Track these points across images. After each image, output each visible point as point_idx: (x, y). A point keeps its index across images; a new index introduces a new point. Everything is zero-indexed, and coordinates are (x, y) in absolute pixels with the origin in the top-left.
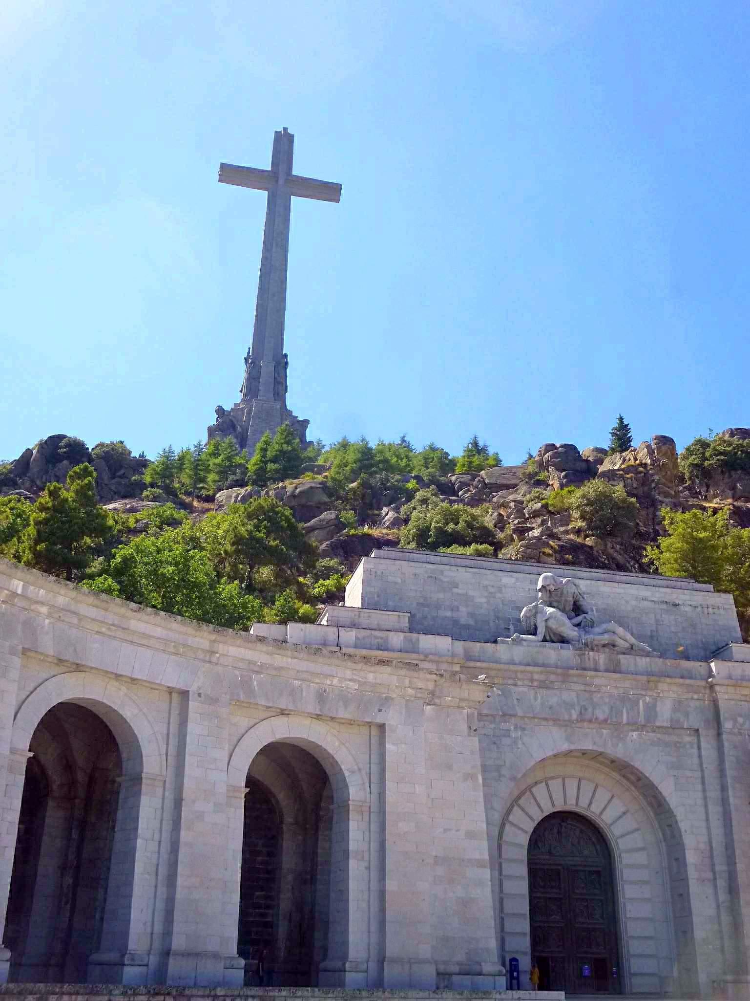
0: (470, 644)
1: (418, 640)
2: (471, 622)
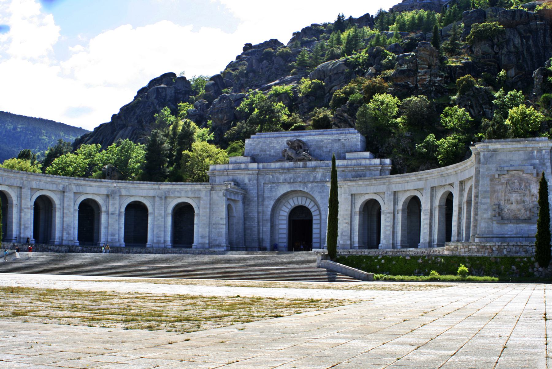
0: (264, 164)
2: (274, 154)
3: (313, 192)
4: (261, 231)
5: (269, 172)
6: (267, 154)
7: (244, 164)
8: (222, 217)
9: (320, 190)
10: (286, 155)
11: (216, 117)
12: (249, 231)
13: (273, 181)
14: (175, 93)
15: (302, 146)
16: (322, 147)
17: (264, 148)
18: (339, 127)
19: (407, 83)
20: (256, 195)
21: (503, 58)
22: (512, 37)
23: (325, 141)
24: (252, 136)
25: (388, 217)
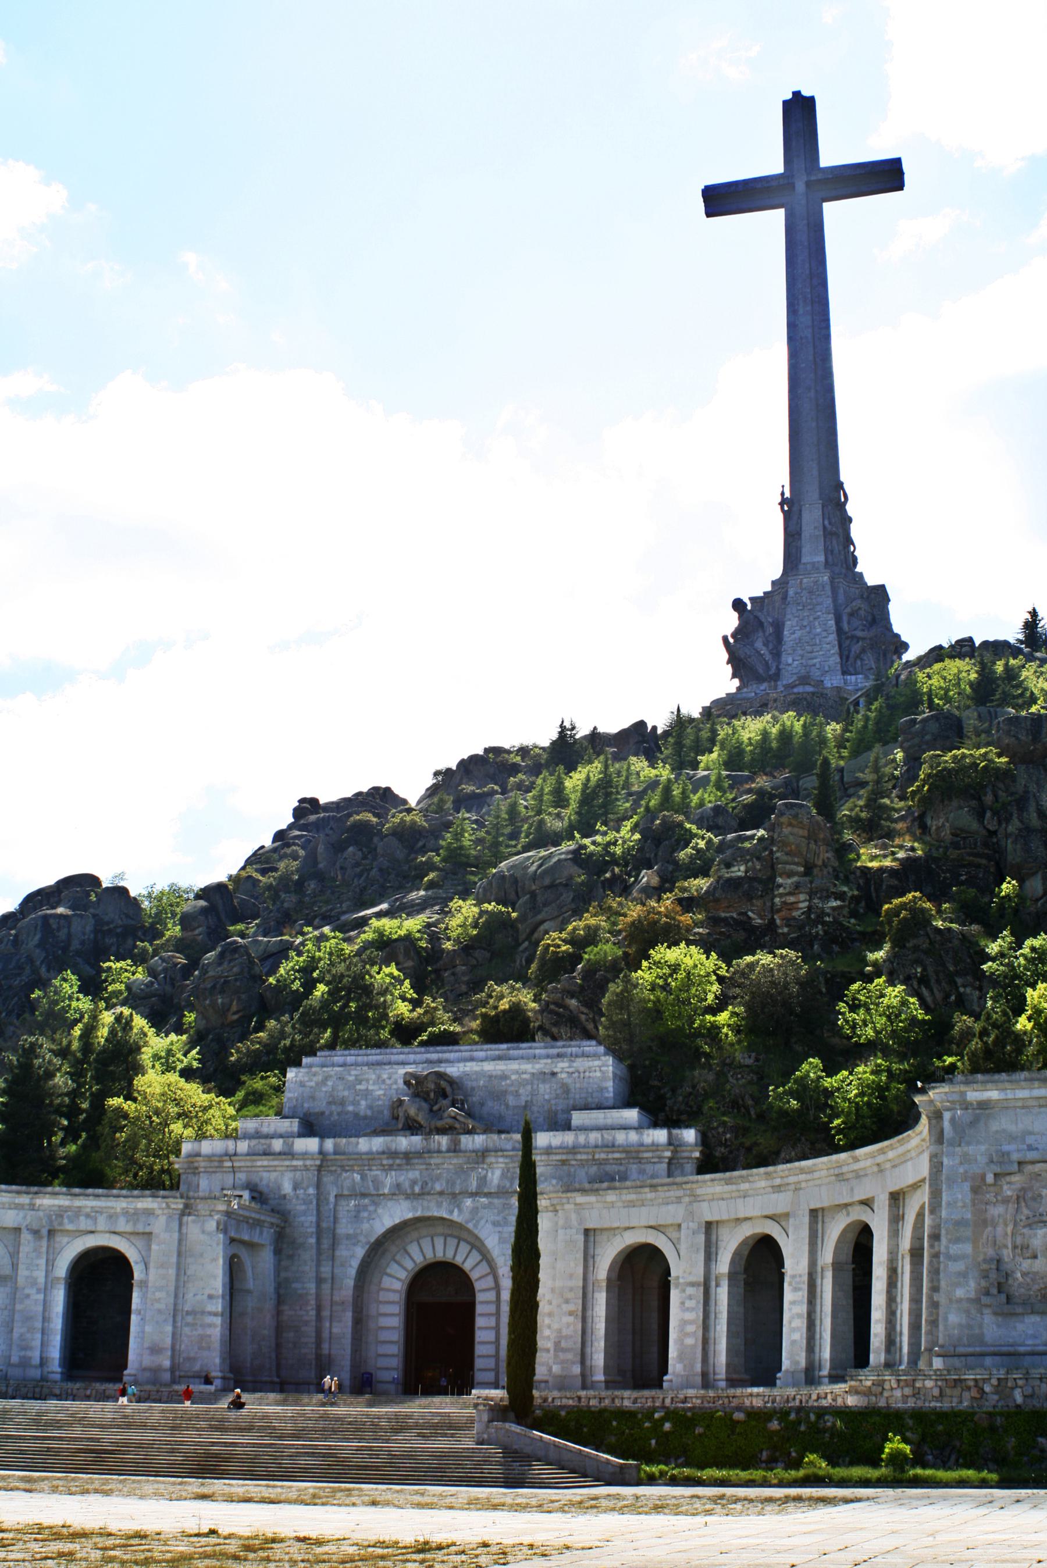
0: (338, 1140)
1: (293, 1143)
2: (369, 1113)
3: (478, 1222)
4: (326, 1335)
5: (351, 1163)
6: (347, 1113)
7: (281, 1141)
8: (213, 1292)
9: (497, 1218)
10: (401, 1114)
11: (207, 1002)
12: (292, 1334)
13: (363, 1190)
14: (96, 931)
15: (448, 1090)
16: (505, 1093)
17: (341, 1094)
18: (554, 1038)
19: (745, 914)
20: (314, 1230)
21: (1009, 846)
22: (1033, 788)
23: (513, 1077)
24: (305, 1060)
25: (690, 1298)
